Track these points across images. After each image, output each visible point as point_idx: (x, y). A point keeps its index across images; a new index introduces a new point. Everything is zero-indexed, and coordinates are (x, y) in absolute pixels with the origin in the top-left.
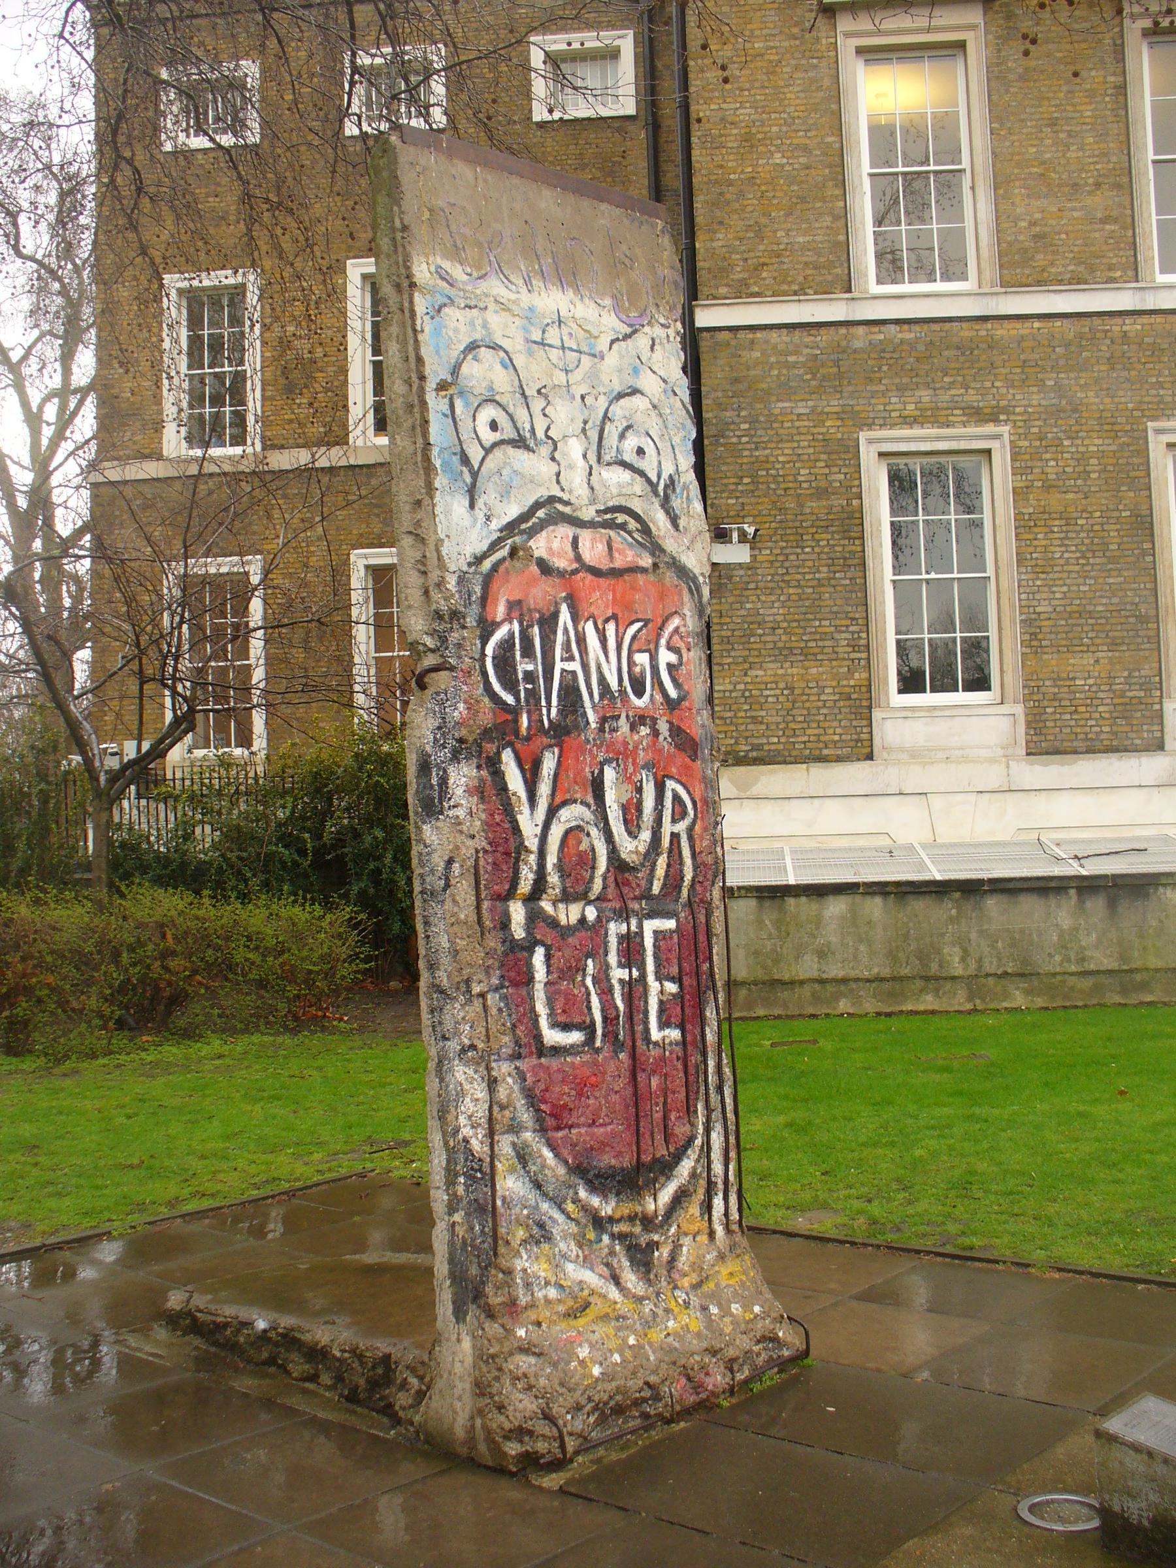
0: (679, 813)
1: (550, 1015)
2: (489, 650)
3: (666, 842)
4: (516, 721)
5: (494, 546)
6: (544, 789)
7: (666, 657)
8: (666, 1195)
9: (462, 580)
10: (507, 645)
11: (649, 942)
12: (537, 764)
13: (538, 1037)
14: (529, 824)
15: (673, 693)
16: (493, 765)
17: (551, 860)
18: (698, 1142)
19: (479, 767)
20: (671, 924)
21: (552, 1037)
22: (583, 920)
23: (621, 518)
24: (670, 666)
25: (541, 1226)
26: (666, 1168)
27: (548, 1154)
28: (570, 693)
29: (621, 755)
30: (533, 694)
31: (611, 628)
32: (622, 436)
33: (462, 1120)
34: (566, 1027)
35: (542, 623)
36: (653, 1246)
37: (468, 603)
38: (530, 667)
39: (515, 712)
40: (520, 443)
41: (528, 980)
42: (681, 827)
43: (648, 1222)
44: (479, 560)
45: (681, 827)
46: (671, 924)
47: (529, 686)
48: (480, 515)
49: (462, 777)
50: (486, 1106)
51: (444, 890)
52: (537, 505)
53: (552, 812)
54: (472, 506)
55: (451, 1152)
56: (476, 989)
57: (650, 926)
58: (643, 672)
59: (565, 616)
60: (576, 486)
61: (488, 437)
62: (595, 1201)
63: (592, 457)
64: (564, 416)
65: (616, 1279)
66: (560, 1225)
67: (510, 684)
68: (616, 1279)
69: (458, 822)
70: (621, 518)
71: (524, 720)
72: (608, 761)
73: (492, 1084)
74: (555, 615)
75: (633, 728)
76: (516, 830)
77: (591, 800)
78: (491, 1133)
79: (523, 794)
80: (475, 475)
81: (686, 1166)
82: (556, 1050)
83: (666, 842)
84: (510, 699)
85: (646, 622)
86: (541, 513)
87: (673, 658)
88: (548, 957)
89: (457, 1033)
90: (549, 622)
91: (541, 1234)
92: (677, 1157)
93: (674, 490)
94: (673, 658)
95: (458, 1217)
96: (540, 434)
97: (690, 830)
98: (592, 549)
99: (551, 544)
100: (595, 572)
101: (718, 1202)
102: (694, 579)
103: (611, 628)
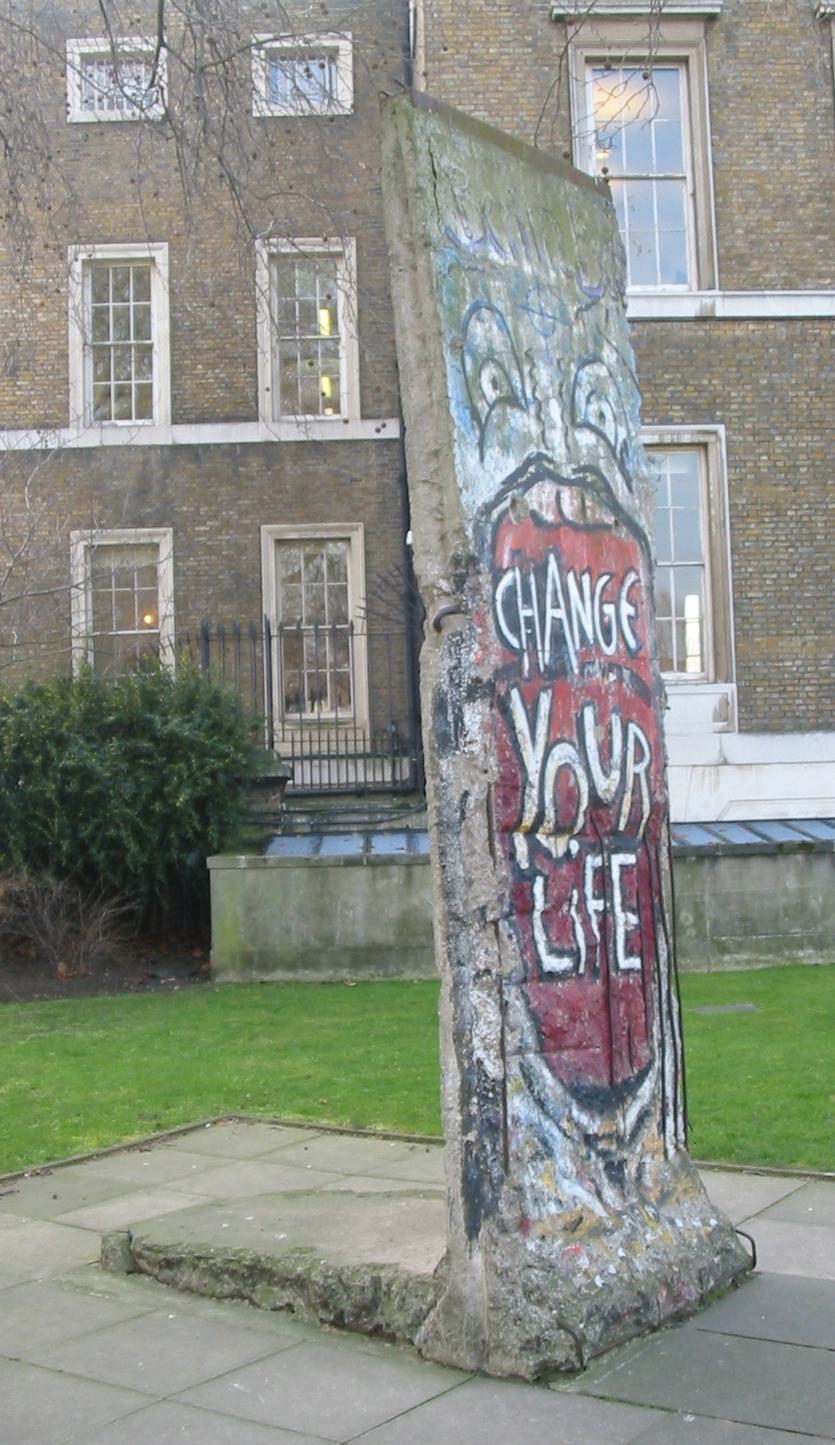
0: (639, 756)
1: (549, 941)
2: (499, 596)
4: (521, 662)
5: (499, 498)
9: (477, 529)
10: (511, 591)
11: (616, 875)
13: (538, 962)
14: (532, 759)
15: (632, 643)
16: (503, 706)
17: (549, 796)
18: (657, 1064)
19: (491, 706)
21: (551, 963)
22: (568, 853)
24: (630, 617)
25: (545, 1143)
26: (631, 1087)
27: (547, 1073)
28: (558, 639)
30: (531, 637)
31: (586, 579)
33: (476, 1042)
34: (560, 954)
37: (481, 551)
38: (528, 613)
44: (488, 508)
45: (641, 768)
47: (529, 631)
49: (475, 716)
50: (499, 1028)
51: (460, 822)
52: (529, 462)
54: (482, 458)
55: (466, 1073)
56: (491, 916)
58: (610, 622)
62: (584, 1119)
65: (599, 1194)
66: (559, 1144)
67: (515, 629)
68: (599, 1194)
69: (473, 757)
72: (588, 704)
73: (504, 1007)
74: (546, 563)
75: (604, 674)
77: (576, 741)
78: (503, 1054)
79: (527, 732)
81: (647, 1089)
82: (552, 976)
84: (514, 642)
85: (612, 576)
86: (532, 469)
88: (546, 887)
89: (472, 958)
91: (545, 1151)
92: (641, 1078)
93: (627, 454)
95: (471, 1137)
96: (529, 395)
97: (647, 770)
103: (586, 579)
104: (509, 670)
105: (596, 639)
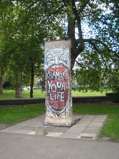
3: (62, 87)
6: (51, 83)
7: (64, 74)
8: (61, 112)
9: (46, 70)
10: (49, 74)
12: (51, 81)
14: (50, 85)
15: (64, 76)
16: (47, 81)
17: (51, 88)
20: (64, 93)
21: (51, 99)
23: (60, 64)
26: (62, 110)
27: (50, 106)
28: (54, 77)
29: (58, 81)
30: (51, 77)
31: (58, 72)
32: (62, 58)
35: (52, 72)
36: (60, 115)
39: (49, 78)
40: (52, 60)
41: (50, 95)
42: (64, 86)
43: (59, 113)
44: (47, 69)
46: (64, 93)
48: (48, 66)
52: (53, 64)
53: (52, 85)
57: (62, 93)
59: (54, 71)
60: (57, 63)
61: (49, 60)
62: (53, 110)
63: (58, 60)
64: (56, 58)
65: (55, 116)
68: (55, 116)
70: (60, 64)
71: (50, 79)
74: (53, 72)
76: (49, 86)
80: (48, 63)
81: (63, 110)
82: (52, 100)
83: (62, 87)
84: (49, 77)
87: (65, 74)
90: (53, 72)
91: (49, 111)
94: (65, 74)
96: (54, 59)
97: (65, 86)
98: (57, 67)
99: (54, 67)
100: (57, 68)
101: (67, 114)
102: (68, 68)
103: (58, 72)
104: (48, 79)
105: (59, 76)
